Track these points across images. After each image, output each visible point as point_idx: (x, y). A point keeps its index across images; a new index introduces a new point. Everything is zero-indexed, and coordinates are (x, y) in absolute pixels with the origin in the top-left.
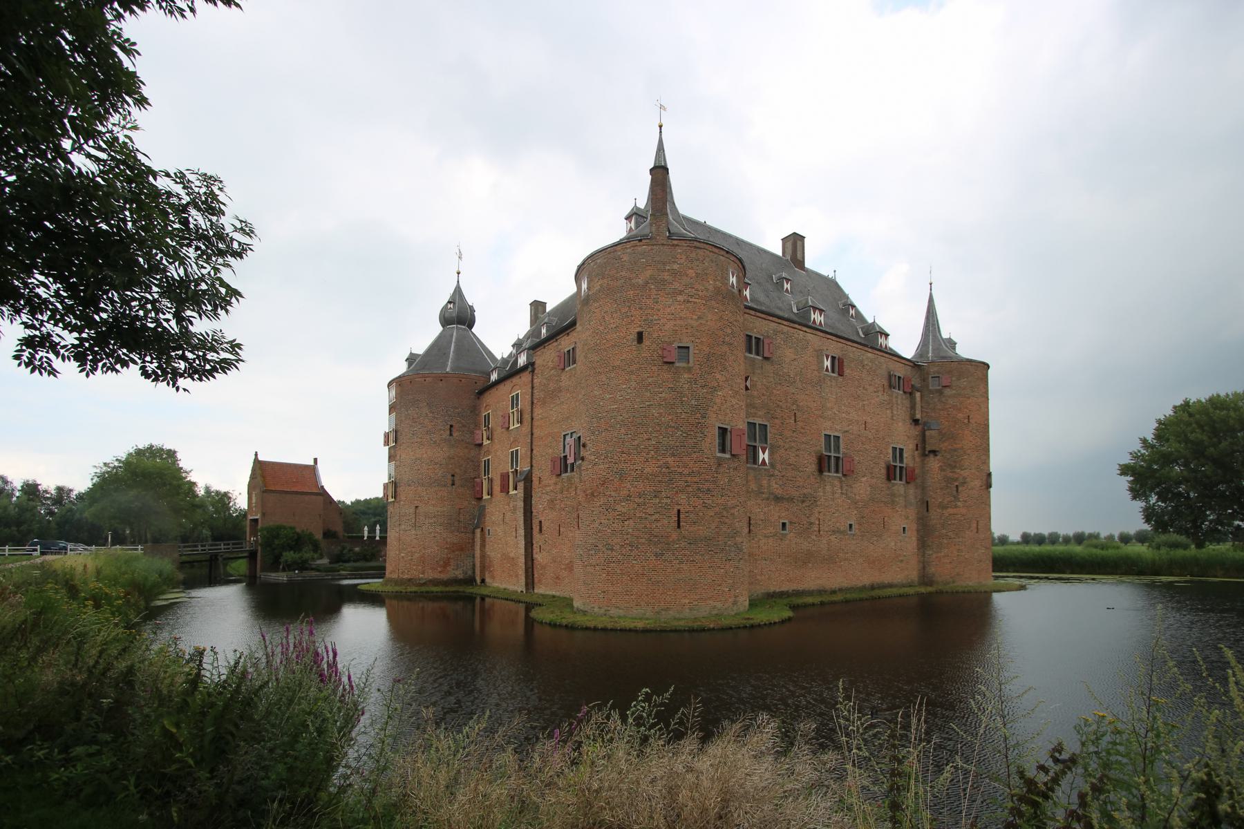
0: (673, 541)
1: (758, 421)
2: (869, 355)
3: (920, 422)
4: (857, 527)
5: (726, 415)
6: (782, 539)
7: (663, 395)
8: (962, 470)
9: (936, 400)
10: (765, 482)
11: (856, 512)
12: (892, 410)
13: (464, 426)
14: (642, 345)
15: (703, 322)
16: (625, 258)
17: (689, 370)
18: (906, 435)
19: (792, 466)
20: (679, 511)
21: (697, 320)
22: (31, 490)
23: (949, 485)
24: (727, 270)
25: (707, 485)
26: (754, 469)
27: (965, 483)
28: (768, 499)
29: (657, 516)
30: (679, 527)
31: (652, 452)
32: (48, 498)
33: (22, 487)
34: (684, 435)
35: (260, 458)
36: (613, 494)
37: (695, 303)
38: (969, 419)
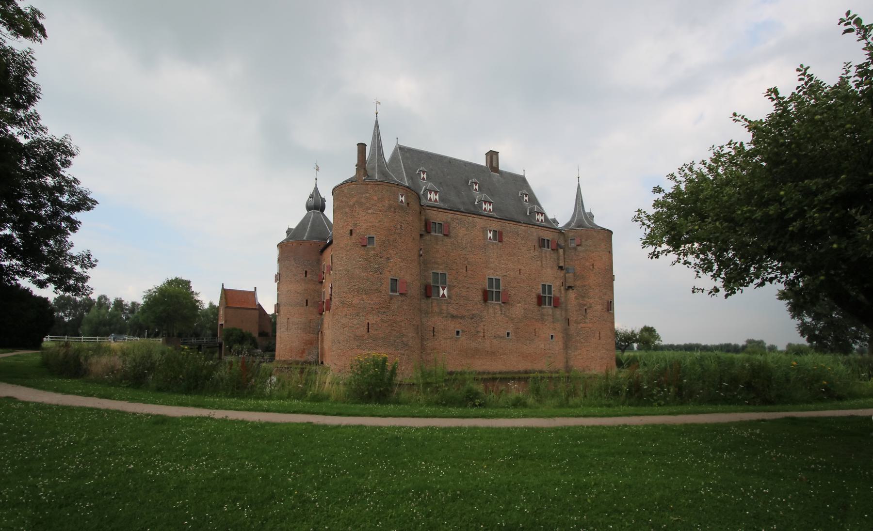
1: (440, 272)
3: (563, 268)
4: (513, 334)
5: (396, 272)
6: (456, 341)
7: (361, 263)
8: (589, 299)
9: (573, 254)
11: (512, 325)
12: (542, 261)
13: (313, 271)
14: (352, 237)
15: (382, 223)
16: (346, 191)
17: (374, 249)
18: (554, 277)
19: (464, 298)
21: (378, 223)
22: (119, 303)
23: (581, 309)
24: (398, 194)
25: (384, 310)
26: (437, 300)
27: (591, 307)
31: (356, 293)
32: (126, 309)
33: (114, 302)
35: (225, 288)
37: (377, 214)
38: (593, 266)
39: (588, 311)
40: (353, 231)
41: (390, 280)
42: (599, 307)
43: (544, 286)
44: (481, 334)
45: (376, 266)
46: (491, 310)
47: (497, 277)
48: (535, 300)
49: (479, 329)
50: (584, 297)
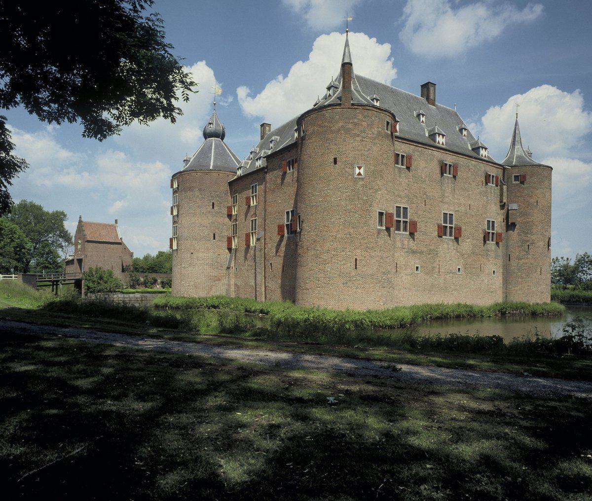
0: (353, 276)
1: (402, 206)
2: (473, 162)
7: (348, 194)
10: (406, 242)
20: (356, 259)
25: (372, 245)
28: (407, 252)
29: (344, 262)
30: (356, 268)
34: (359, 216)
36: (319, 249)
37: (366, 141)
39: (530, 247)
40: (338, 159)
41: (378, 213)
42: (541, 243)
43: (489, 221)
44: (437, 270)
45: (365, 198)
46: (445, 246)
47: (451, 213)
48: (482, 236)
49: (435, 265)
50: (527, 233)
